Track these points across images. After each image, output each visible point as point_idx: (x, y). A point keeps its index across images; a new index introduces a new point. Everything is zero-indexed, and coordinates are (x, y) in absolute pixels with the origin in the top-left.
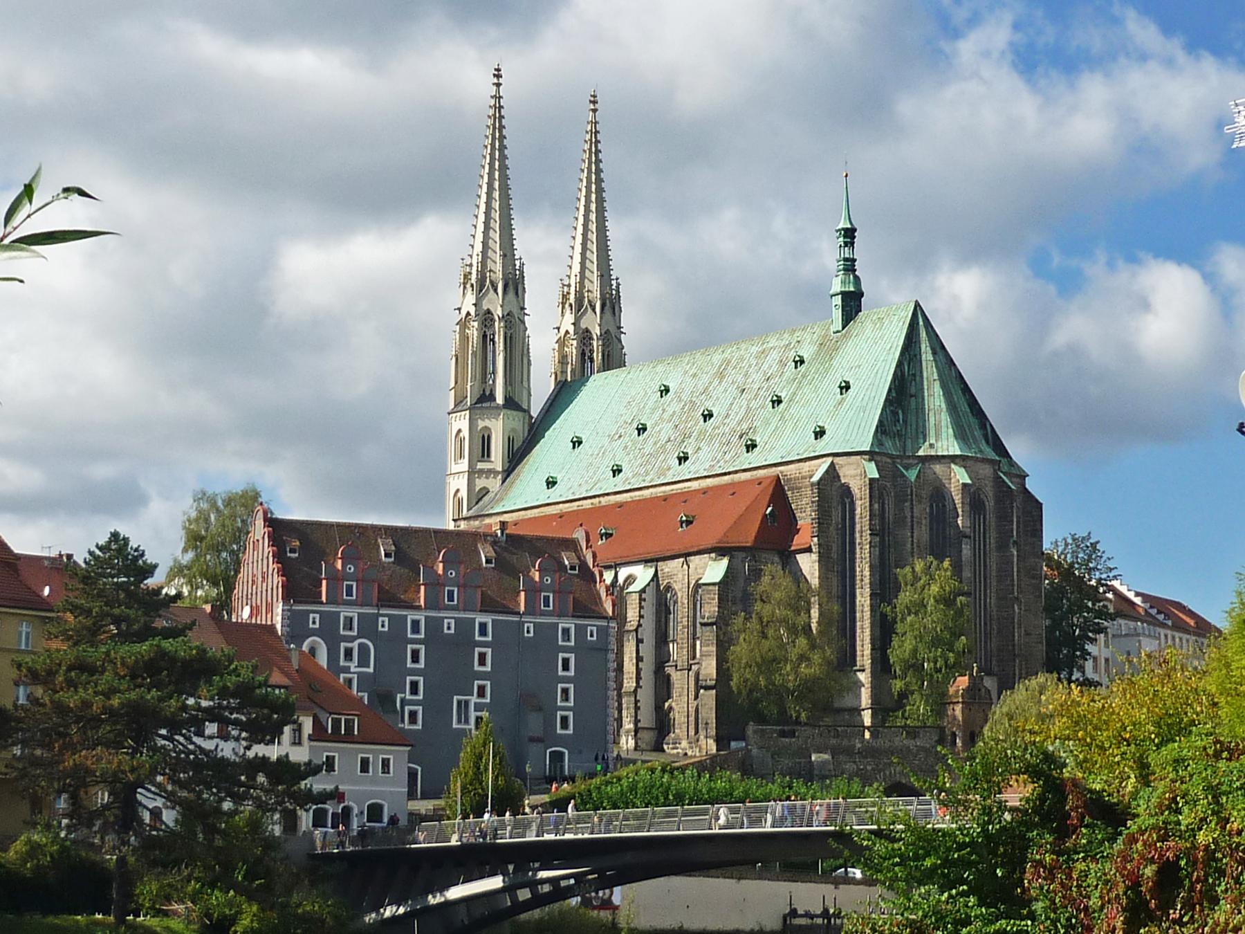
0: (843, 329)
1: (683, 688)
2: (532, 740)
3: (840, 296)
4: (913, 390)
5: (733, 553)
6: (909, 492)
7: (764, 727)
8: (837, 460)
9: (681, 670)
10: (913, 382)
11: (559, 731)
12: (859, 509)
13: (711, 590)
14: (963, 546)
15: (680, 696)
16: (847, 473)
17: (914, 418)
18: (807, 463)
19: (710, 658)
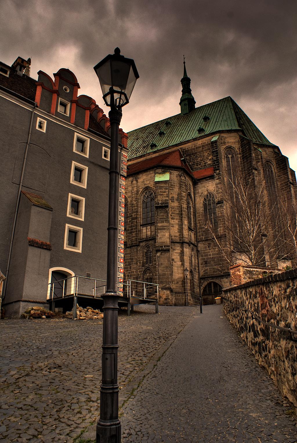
0: (189, 112)
1: (132, 259)
2: (33, 244)
3: (187, 101)
4: (242, 123)
5: (171, 171)
6: (260, 157)
7: (252, 269)
8: (222, 135)
9: (128, 247)
10: (241, 120)
11: (66, 247)
12: (239, 160)
13: (162, 187)
14: (291, 189)
15: (130, 264)
16: (230, 141)
17: (247, 132)
18: (200, 141)
19: (164, 231)
